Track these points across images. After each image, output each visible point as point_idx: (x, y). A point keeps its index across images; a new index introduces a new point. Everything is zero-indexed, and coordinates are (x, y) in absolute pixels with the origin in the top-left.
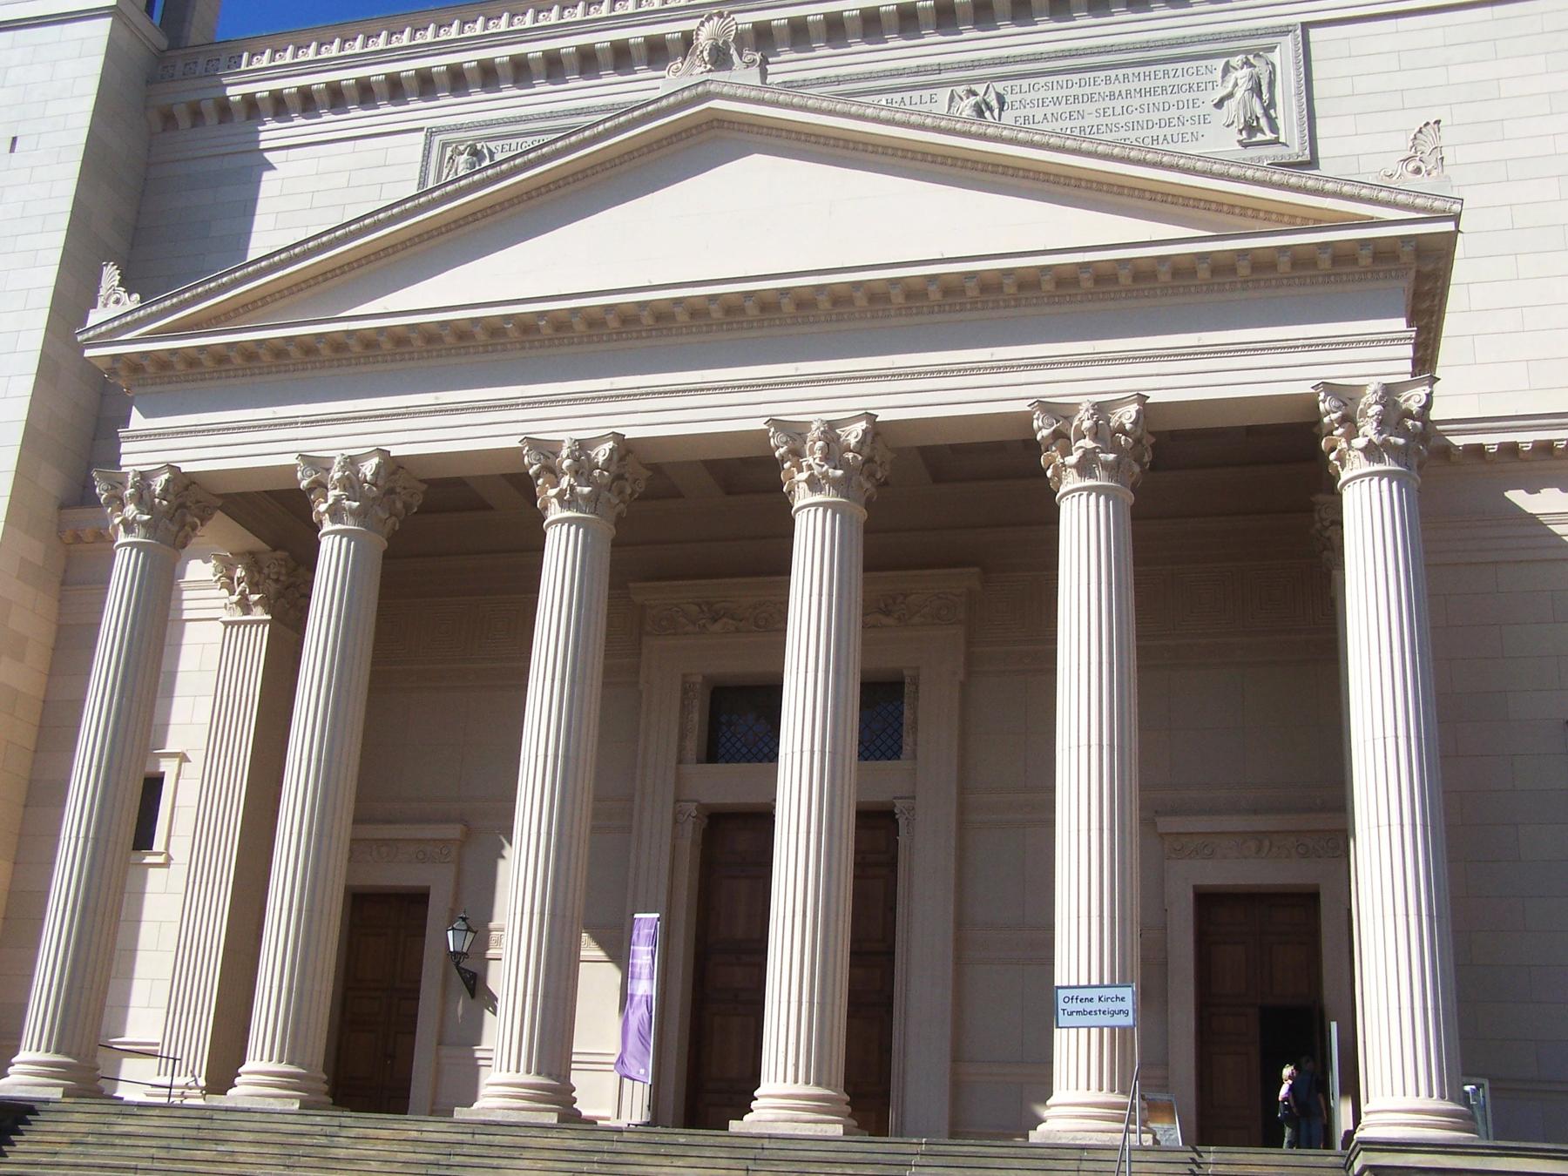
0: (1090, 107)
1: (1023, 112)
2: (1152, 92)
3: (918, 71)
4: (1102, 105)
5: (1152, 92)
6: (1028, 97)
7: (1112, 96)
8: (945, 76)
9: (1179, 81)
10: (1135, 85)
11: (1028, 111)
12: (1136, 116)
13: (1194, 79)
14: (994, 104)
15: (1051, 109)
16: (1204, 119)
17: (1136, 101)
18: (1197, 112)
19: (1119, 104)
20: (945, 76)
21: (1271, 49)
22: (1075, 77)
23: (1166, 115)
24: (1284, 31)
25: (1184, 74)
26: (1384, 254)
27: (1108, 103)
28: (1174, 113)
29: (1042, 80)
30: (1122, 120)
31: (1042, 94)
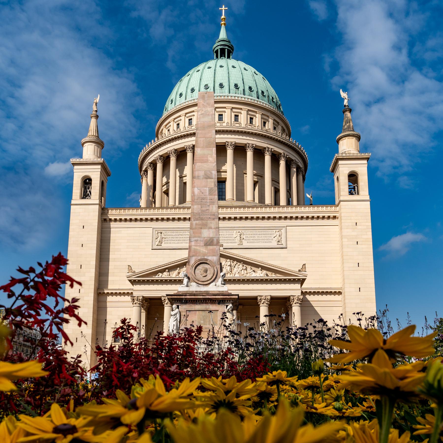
0: (256, 236)
1: (246, 236)
2: (265, 234)
3: (231, 227)
4: (258, 236)
5: (265, 234)
6: (247, 233)
7: (259, 234)
8: (235, 229)
9: (269, 233)
10: (262, 233)
11: (247, 236)
12: (263, 238)
13: (271, 233)
14: (242, 234)
15: (251, 236)
16: (272, 240)
17: (263, 236)
18: (272, 238)
19: (260, 236)
20: (235, 229)
21: (282, 229)
22: (254, 231)
23: (267, 238)
24: (284, 227)
25: (270, 232)
26: (299, 279)
27: (259, 236)
28: (268, 238)
29: (249, 231)
30: (261, 238)
31: (249, 233)
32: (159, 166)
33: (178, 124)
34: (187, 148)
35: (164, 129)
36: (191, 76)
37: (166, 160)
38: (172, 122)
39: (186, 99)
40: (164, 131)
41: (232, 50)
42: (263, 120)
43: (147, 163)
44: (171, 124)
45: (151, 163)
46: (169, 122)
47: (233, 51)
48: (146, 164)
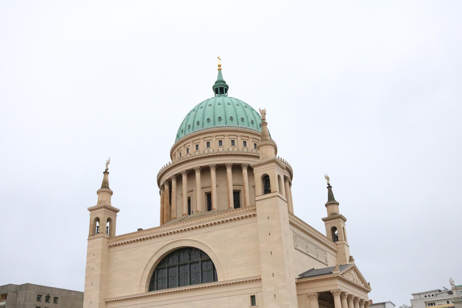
32: (174, 183)
33: (188, 149)
34: (195, 169)
35: (177, 153)
36: (197, 111)
37: (179, 177)
38: (183, 148)
39: (193, 130)
40: (176, 154)
41: (227, 88)
42: (254, 143)
43: (164, 180)
44: (182, 148)
45: (167, 180)
46: (181, 147)
47: (228, 89)
48: (163, 181)
